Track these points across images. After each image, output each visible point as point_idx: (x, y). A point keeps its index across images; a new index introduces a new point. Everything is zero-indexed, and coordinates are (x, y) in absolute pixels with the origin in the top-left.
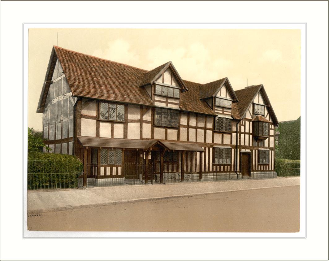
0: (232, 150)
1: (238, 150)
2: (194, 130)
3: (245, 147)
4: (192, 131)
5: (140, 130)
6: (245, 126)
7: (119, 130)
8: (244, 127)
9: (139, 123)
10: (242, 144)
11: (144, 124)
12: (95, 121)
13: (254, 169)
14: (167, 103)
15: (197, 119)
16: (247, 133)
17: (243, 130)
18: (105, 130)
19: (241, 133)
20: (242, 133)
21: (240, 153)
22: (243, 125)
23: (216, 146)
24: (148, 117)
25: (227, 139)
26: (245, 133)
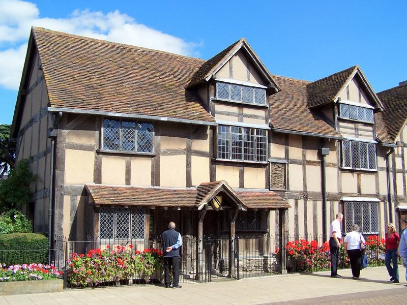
0: (379, 205)
2: (300, 167)
4: (295, 172)
5: (187, 170)
7: (141, 170)
8: (401, 158)
11: (195, 159)
12: (93, 154)
14: (241, 116)
17: (399, 166)
18: (114, 172)
19: (395, 171)
21: (397, 210)
23: (345, 199)
24: (204, 145)
25: (368, 183)
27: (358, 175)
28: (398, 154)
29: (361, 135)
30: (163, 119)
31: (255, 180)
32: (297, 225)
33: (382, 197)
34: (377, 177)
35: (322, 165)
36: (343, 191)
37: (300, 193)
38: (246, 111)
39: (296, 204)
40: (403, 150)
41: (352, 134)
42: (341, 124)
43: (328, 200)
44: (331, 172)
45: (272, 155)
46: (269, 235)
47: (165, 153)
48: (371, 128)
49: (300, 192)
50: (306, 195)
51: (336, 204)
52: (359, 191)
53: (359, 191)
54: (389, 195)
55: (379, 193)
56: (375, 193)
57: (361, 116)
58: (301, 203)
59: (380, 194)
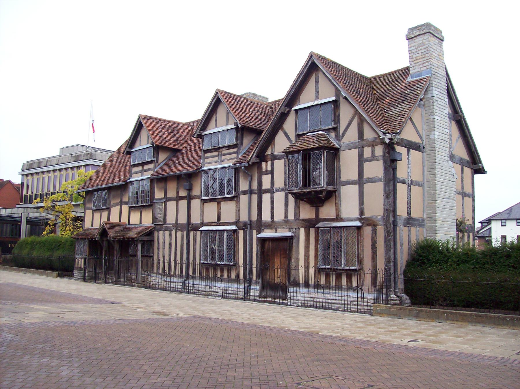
1: (255, 232)
2: (175, 203)
3: (272, 225)
4: (171, 206)
6: (272, 173)
8: (270, 175)
9: (119, 207)
10: (266, 217)
13: (302, 280)
15: (178, 184)
16: (278, 191)
19: (261, 192)
20: (267, 191)
22: (266, 173)
25: (228, 211)
26: (270, 191)
27: (219, 203)
28: (266, 171)
29: (224, 161)
30: (103, 187)
31: (147, 218)
32: (170, 252)
33: (241, 225)
34: (238, 202)
35: (189, 198)
37: (173, 226)
38: (146, 167)
39: (170, 235)
40: (272, 165)
41: (217, 162)
42: (207, 155)
43: (191, 230)
44: (196, 203)
45: (156, 197)
46: (153, 259)
47: (113, 206)
48: (235, 150)
50: (177, 227)
51: (198, 233)
52: (219, 219)
53: (219, 219)
55: (239, 220)
56: (234, 220)
57: (224, 139)
58: (173, 233)
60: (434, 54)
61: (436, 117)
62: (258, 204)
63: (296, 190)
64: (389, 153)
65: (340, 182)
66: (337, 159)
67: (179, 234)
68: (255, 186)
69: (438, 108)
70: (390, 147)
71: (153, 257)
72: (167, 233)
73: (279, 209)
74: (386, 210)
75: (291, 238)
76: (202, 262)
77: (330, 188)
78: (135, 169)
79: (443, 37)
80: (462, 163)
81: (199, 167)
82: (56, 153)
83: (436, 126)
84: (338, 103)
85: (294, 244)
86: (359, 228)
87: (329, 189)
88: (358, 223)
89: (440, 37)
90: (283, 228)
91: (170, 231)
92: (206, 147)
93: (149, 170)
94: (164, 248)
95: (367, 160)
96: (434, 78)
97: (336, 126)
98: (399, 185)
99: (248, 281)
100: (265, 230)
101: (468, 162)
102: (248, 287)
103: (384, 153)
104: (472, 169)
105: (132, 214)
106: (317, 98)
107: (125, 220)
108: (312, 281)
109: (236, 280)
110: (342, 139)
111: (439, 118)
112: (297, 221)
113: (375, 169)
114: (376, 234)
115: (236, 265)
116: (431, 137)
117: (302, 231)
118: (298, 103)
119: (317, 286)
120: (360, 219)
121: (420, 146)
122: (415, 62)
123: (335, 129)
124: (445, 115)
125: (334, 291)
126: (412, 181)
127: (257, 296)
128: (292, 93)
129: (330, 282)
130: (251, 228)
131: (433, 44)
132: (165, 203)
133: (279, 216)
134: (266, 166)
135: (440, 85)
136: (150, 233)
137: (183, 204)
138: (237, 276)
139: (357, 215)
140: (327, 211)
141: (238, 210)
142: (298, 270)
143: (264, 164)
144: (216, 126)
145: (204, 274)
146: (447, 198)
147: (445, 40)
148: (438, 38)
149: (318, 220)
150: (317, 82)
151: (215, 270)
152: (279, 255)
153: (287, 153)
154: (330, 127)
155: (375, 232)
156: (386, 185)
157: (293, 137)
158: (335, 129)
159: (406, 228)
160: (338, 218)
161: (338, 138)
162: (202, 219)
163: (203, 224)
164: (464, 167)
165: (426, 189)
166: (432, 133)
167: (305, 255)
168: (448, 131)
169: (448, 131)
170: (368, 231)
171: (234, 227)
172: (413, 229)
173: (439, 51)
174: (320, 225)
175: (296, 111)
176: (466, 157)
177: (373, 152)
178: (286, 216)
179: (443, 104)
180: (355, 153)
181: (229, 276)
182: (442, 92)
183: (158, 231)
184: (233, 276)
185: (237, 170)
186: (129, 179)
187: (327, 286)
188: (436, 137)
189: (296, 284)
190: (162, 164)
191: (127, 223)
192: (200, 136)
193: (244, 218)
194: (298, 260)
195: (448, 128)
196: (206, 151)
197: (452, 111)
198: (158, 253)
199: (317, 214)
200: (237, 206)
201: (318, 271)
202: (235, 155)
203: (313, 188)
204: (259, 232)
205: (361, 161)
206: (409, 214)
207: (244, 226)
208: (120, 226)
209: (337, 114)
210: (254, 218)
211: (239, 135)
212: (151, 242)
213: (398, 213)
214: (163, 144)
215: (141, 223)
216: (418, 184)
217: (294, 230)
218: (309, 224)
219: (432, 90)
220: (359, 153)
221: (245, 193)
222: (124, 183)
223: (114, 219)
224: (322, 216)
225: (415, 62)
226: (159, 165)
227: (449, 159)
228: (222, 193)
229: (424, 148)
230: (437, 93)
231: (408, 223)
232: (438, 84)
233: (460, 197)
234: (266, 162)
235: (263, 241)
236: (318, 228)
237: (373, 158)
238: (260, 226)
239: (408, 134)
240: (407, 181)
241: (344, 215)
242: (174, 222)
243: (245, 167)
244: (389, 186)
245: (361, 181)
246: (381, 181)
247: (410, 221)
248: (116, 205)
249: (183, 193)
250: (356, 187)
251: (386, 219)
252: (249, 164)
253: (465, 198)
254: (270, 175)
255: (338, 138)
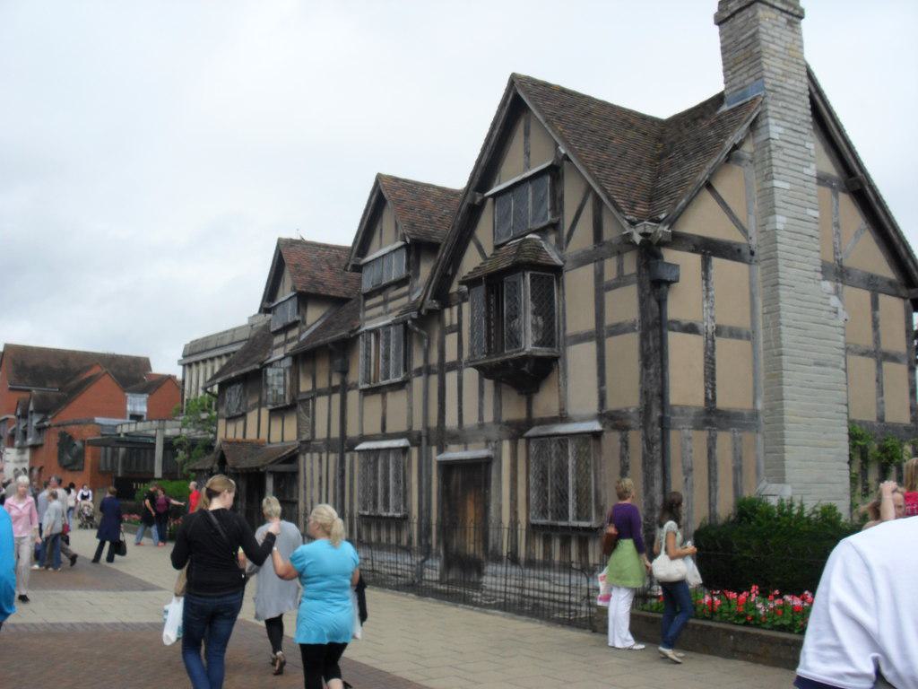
1: (434, 449)
4: (322, 403)
6: (458, 328)
8: (456, 334)
9: (256, 411)
10: (451, 421)
12: (224, 421)
17: (451, 355)
19: (444, 368)
22: (452, 329)
26: (455, 366)
30: (233, 375)
33: (415, 437)
35: (344, 389)
36: (367, 432)
38: (292, 334)
39: (320, 460)
41: (380, 315)
42: (369, 303)
43: (347, 451)
44: (353, 396)
45: (302, 390)
48: (406, 289)
49: (323, 440)
50: (329, 445)
51: (356, 455)
54: (427, 429)
55: (410, 428)
56: (404, 428)
59: (414, 429)
60: (772, 46)
61: (776, 183)
62: (439, 394)
63: (483, 359)
64: (647, 266)
65: (565, 338)
66: (558, 286)
67: (332, 457)
68: (434, 358)
69: (784, 165)
70: (649, 251)
71: (296, 503)
72: (316, 456)
73: (470, 401)
74: (645, 394)
75: (487, 462)
76: (361, 512)
77: (543, 352)
78: (279, 339)
79: (802, 11)
80: (872, 284)
81: (355, 327)
82: (245, 322)
83: (778, 203)
84: (560, 171)
85: (494, 475)
86: (596, 435)
87: (539, 354)
88: (596, 426)
89: (791, 10)
90: (477, 441)
91: (320, 453)
92: (367, 286)
93: (293, 339)
94: (312, 486)
95: (610, 287)
96: (773, 98)
97: (555, 220)
98: (675, 340)
99: (427, 552)
100: (452, 447)
101: (891, 283)
102: (423, 561)
103: (639, 267)
104: (904, 298)
105: (272, 423)
106: (528, 167)
107: (264, 435)
108: (522, 553)
109: (407, 550)
110: (567, 246)
111: (787, 186)
112: (499, 426)
113: (625, 305)
114: (627, 447)
115: (406, 518)
116: (768, 228)
117: (506, 446)
118: (497, 181)
119: (530, 563)
120: (601, 417)
121: (739, 251)
122: (733, 70)
123: (555, 226)
124: (809, 178)
125: (557, 575)
126: (717, 327)
127: (436, 581)
128: (483, 162)
129: (550, 555)
130: (429, 444)
131: (770, 26)
132: (313, 398)
133: (471, 419)
134: (450, 316)
135: (792, 113)
136: (292, 458)
137: (336, 398)
138: (410, 540)
139: (593, 408)
140: (546, 402)
141: (411, 408)
142: (499, 528)
143: (447, 311)
144: (381, 247)
145: (364, 537)
146: (816, 364)
147: (807, 13)
148: (786, 12)
149: (530, 422)
150: (527, 134)
151: (379, 529)
152: (473, 496)
153: (472, 282)
154: (545, 223)
155: (625, 443)
156: (644, 338)
157: (489, 251)
158: (555, 226)
159: (704, 435)
160: (563, 418)
161: (558, 241)
162: (362, 428)
163: (364, 438)
164: (883, 298)
165: (761, 346)
166: (771, 218)
167: (511, 499)
168: (816, 214)
169: (816, 214)
170: (612, 440)
171: (402, 443)
172: (724, 440)
173: (790, 40)
174: (532, 432)
175: (495, 196)
176: (885, 271)
177: (620, 268)
178: (481, 418)
179: (801, 156)
180: (588, 271)
181: (399, 541)
182: (795, 127)
183: (304, 454)
184: (404, 542)
185: (407, 331)
186: (269, 358)
187: (547, 564)
188: (779, 226)
189: (497, 559)
190: (314, 328)
191: (267, 440)
192: (358, 269)
193: (418, 426)
194: (500, 508)
195: (815, 206)
196: (368, 296)
197: (839, 172)
198: (305, 494)
199: (529, 412)
200: (408, 400)
201: (533, 529)
202: (405, 300)
203: (510, 354)
204: (441, 450)
205: (601, 288)
206: (710, 401)
207: (416, 439)
208: (256, 446)
209: (559, 195)
210: (433, 422)
211: (412, 258)
212: (294, 475)
213: (674, 398)
214: (312, 290)
215: (283, 441)
216: (735, 333)
217: (493, 444)
218: (517, 431)
219: (767, 125)
220: (595, 272)
221: (419, 372)
222: (258, 367)
223: (251, 435)
224: (538, 412)
225: (733, 70)
226: (308, 328)
227: (819, 276)
228: (387, 377)
229: (752, 253)
230: (781, 130)
231: (707, 423)
232: (783, 111)
233: (870, 363)
234: (450, 306)
235: (447, 468)
236: (528, 439)
237: (621, 281)
238: (442, 437)
239: (704, 220)
240: (701, 327)
241: (572, 410)
242: (325, 436)
243: (412, 319)
244: (648, 340)
245: (599, 335)
246: (635, 331)
247: (712, 417)
248: (254, 407)
249: (336, 381)
250: (591, 347)
251: (645, 412)
252: (419, 314)
253: (886, 365)
254: (456, 334)
255: (561, 245)
